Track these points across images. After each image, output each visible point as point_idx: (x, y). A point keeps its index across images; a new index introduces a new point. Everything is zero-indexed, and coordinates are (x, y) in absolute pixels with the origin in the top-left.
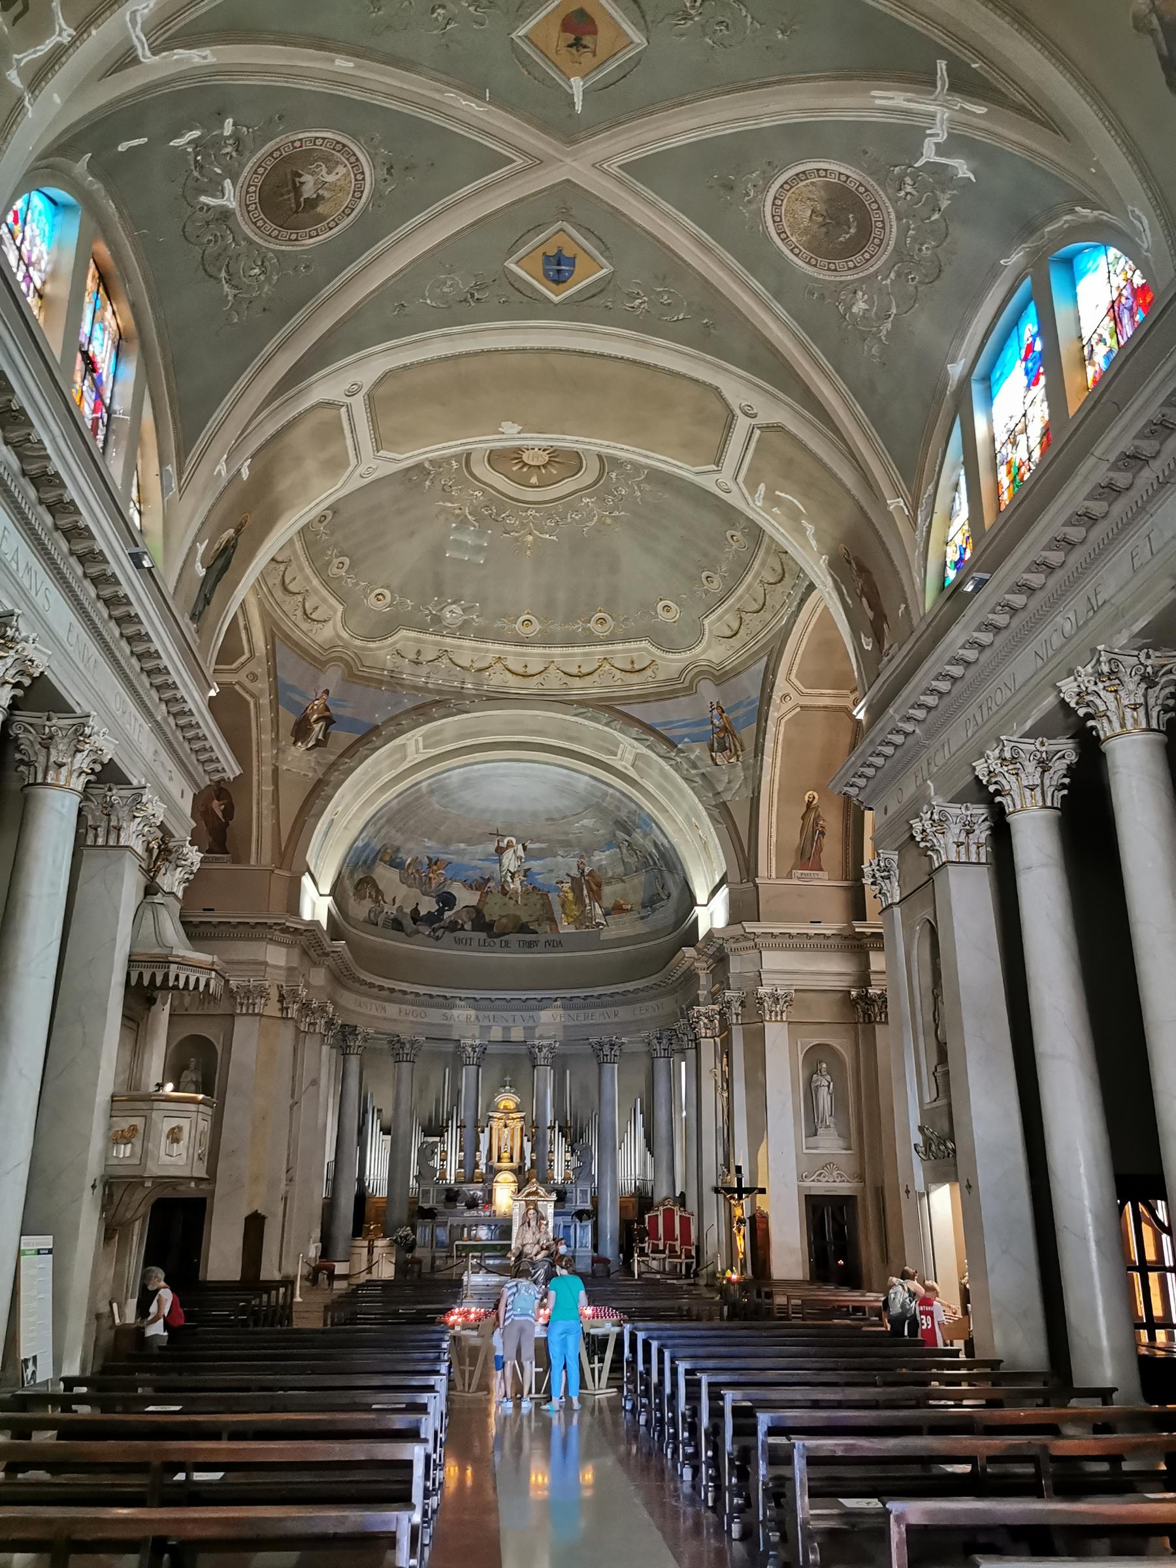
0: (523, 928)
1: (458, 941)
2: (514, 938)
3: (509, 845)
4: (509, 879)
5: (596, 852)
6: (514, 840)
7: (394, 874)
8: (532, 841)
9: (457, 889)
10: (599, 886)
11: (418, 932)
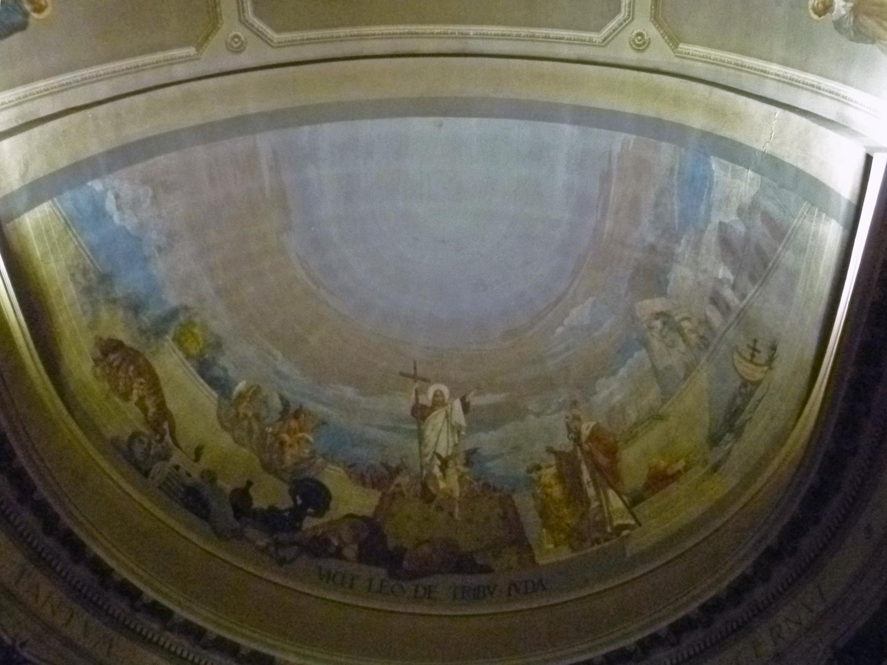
0: (462, 563)
1: (328, 577)
2: (444, 583)
3: (438, 402)
4: (436, 471)
5: (602, 381)
6: (445, 390)
7: (208, 397)
8: (480, 391)
9: (333, 478)
10: (612, 452)
11: (239, 535)
